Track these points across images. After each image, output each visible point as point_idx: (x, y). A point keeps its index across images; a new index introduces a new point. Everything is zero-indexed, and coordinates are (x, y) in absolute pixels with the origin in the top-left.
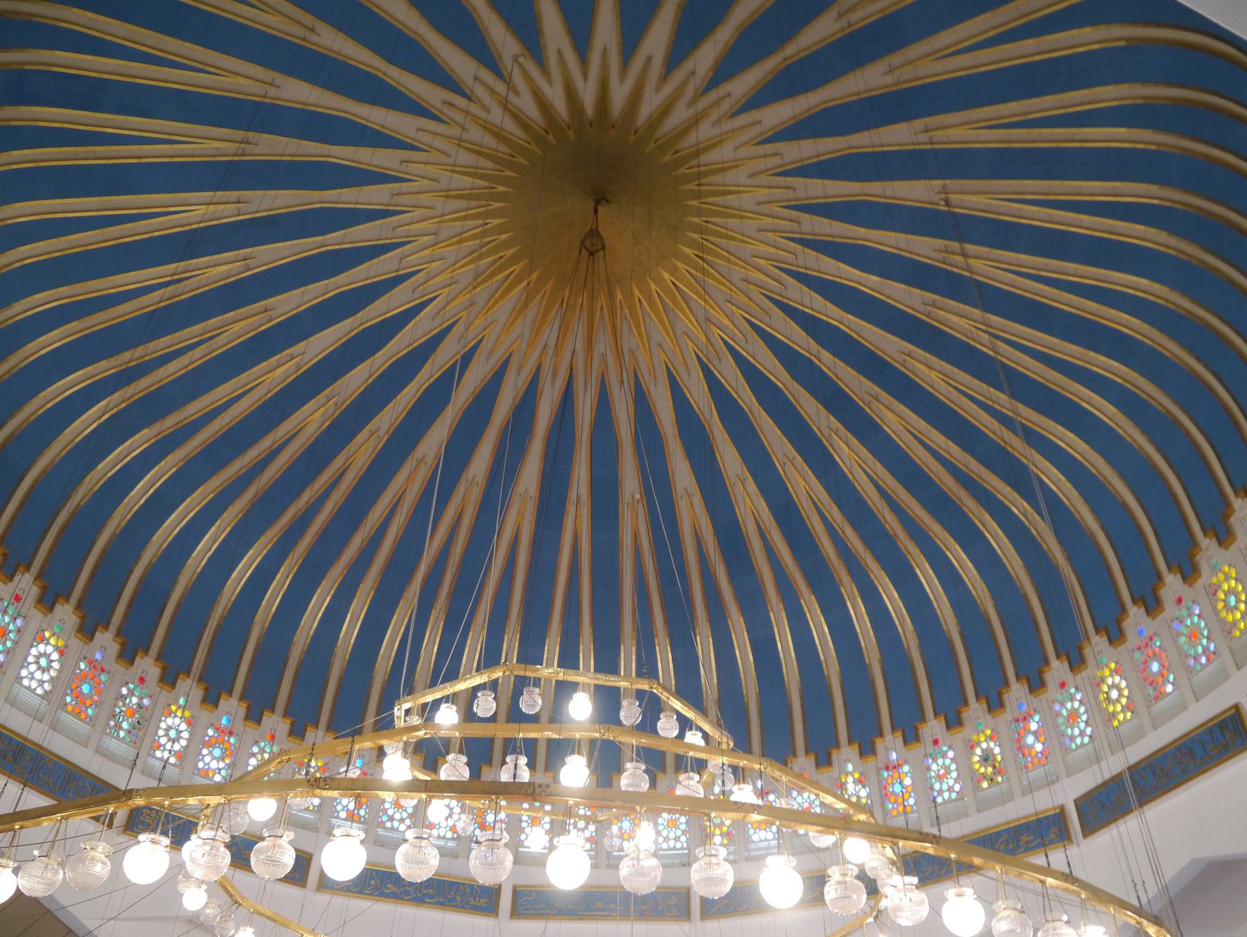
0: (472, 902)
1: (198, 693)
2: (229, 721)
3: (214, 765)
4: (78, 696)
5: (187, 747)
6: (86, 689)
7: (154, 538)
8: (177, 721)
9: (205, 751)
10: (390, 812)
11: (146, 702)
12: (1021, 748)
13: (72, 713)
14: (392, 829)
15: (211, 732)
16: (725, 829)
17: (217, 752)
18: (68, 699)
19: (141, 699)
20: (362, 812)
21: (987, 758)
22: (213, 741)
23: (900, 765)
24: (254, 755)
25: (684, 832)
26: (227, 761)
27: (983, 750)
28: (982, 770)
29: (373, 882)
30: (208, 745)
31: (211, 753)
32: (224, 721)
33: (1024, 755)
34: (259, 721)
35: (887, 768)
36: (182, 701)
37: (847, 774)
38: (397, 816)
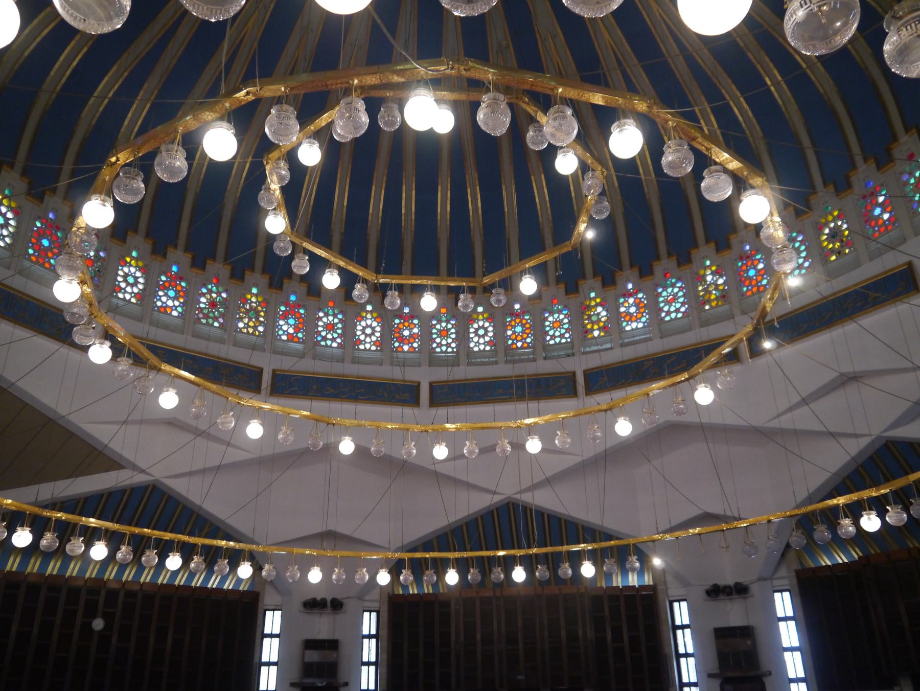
0: (397, 397)
1: (148, 246)
2: (179, 269)
3: (170, 303)
4: (38, 247)
5: (144, 290)
6: (45, 243)
7: (83, 115)
8: (133, 270)
9: (161, 293)
10: (324, 334)
11: (102, 254)
12: (868, 218)
13: (37, 262)
14: (326, 346)
15: (163, 278)
16: (601, 324)
17: (172, 293)
18: (31, 251)
19: (97, 251)
20: (300, 335)
21: (835, 235)
22: (167, 285)
23: (755, 255)
24: (204, 295)
25: (567, 330)
26: (182, 300)
27: (830, 229)
28: (831, 246)
29: (314, 387)
30: (164, 288)
31: (166, 295)
32: (174, 269)
33: (870, 225)
34: (203, 268)
35: (741, 258)
36: (134, 254)
37: (706, 268)
38: (329, 336)
